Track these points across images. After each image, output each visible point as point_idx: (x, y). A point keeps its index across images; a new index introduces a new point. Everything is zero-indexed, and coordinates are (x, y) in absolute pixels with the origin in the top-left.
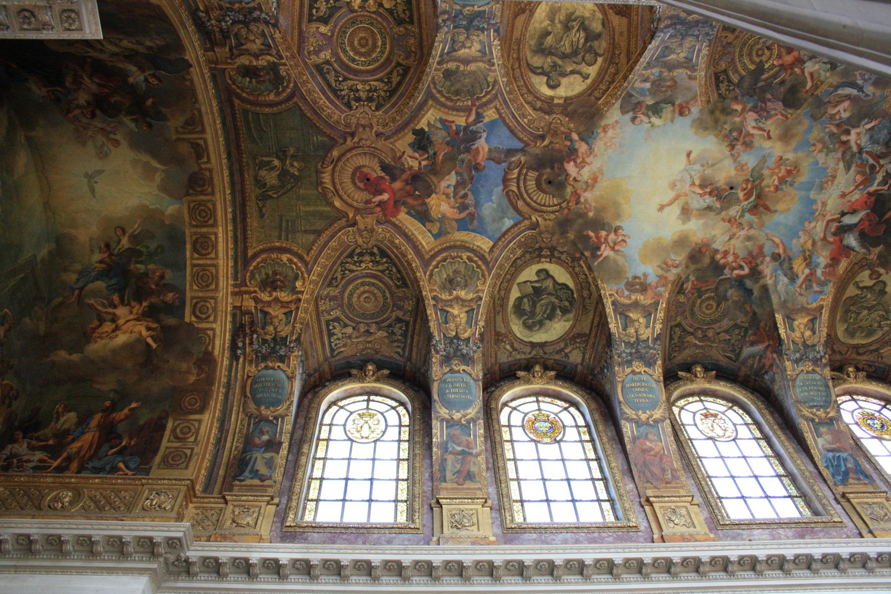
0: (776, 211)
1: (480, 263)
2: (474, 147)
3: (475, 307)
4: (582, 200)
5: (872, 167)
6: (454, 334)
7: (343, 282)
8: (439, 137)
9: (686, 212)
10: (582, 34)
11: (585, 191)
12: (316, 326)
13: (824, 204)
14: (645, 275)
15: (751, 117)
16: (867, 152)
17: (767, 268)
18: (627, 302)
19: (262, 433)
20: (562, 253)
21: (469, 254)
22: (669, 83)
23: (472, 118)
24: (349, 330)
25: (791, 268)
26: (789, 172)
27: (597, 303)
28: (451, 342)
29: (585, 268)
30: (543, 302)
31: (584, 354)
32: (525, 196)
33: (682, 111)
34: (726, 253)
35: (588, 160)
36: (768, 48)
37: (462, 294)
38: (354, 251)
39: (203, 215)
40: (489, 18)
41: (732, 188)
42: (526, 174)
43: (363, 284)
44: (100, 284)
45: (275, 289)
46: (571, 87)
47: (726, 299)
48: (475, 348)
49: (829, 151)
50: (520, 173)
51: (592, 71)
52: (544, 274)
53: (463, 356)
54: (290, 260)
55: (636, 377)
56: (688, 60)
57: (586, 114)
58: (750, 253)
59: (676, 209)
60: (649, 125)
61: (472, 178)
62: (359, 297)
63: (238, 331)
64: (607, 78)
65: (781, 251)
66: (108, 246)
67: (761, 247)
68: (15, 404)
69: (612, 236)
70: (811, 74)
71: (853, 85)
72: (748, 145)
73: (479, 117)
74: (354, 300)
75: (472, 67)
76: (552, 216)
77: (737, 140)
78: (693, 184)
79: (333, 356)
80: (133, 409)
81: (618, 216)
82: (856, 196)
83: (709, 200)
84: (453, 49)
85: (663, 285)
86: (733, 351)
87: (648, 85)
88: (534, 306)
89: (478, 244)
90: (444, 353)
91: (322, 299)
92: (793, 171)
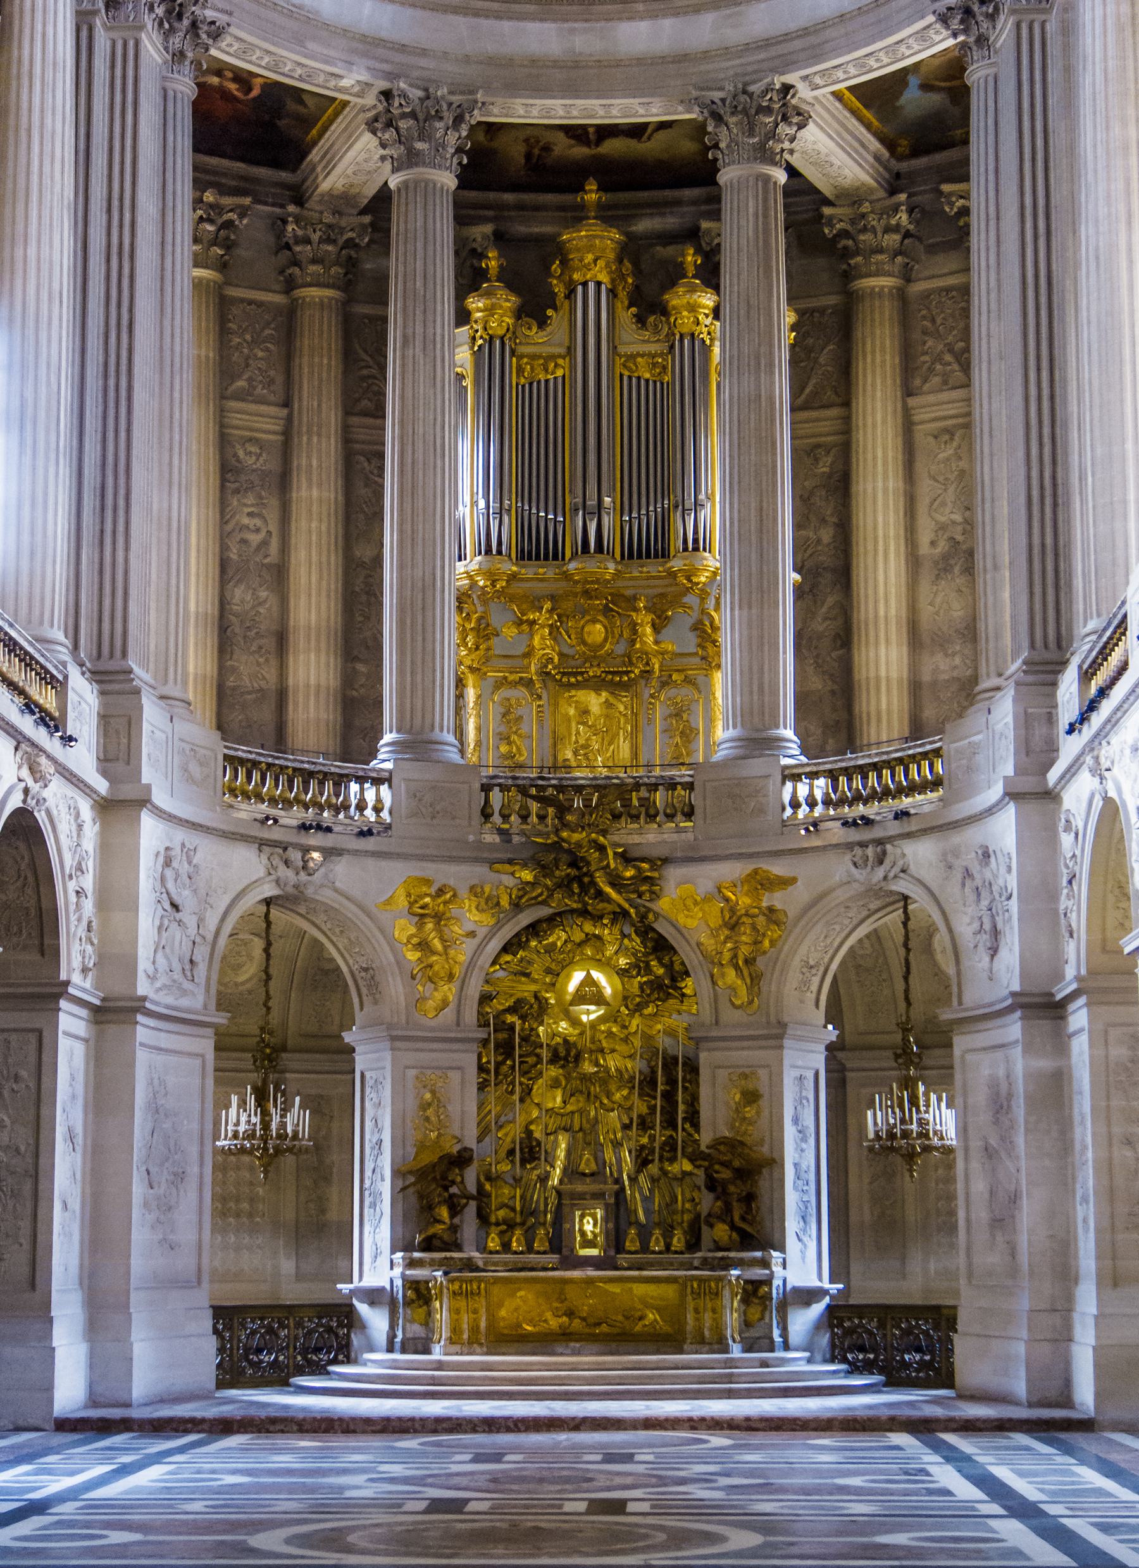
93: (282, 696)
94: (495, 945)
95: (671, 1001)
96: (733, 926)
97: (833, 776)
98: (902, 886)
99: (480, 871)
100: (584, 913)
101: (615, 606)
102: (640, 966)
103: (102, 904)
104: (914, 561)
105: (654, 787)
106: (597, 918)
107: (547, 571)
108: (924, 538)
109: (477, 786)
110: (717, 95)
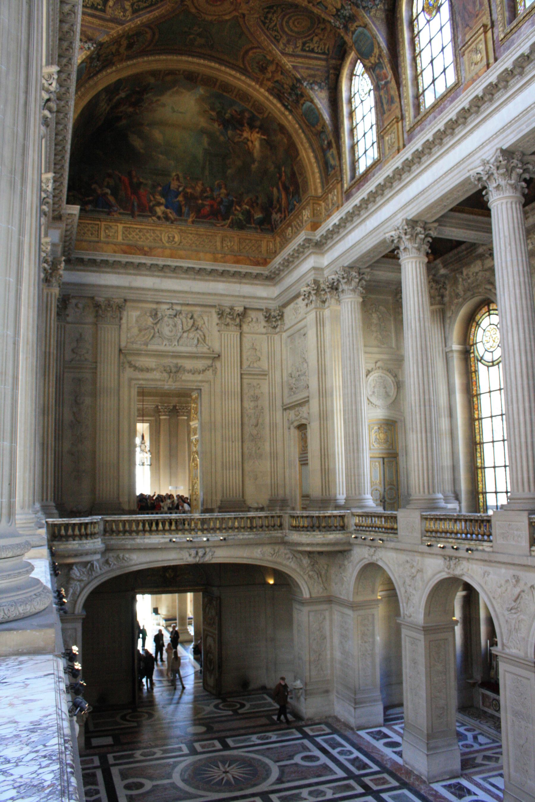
7: (281, 33)
12: (300, 60)
19: (324, 141)
24: (316, 39)
38: (262, 21)
39: (209, 81)
43: (287, 22)
44: (230, 132)
45: (266, 69)
53: (349, 18)
54: (254, 53)
62: (296, 26)
63: (280, 97)
66: (212, 119)
68: (259, 201)
74: (296, 30)
79: (328, 55)
80: (284, 172)
91: (284, 49)
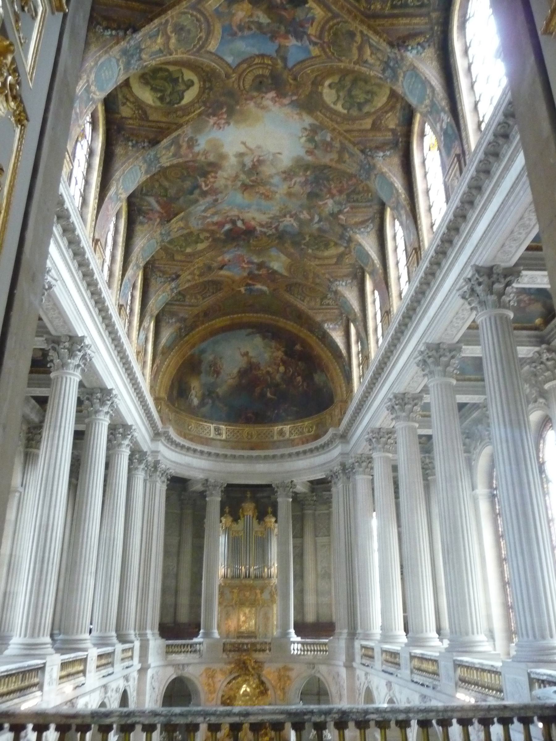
0: (243, 193)
1: (198, 46)
2: (290, 36)
3: (164, 53)
4: (248, 102)
5: (270, 227)
6: (143, 47)
8: (300, 14)
9: (241, 155)
10: (362, 100)
11: (255, 103)
13: (249, 212)
14: (199, 145)
15: (303, 179)
16: (279, 225)
17: (210, 199)
18: (181, 142)
20: (208, 94)
21: (204, 37)
22: (329, 149)
23: (313, 39)
25: (210, 208)
26: (268, 196)
27: (176, 124)
28: (137, 49)
29: (199, 111)
30: (166, 84)
31: (130, 118)
32: (250, 69)
33: (309, 152)
34: (216, 177)
35: (277, 104)
36: (341, 182)
37: (173, 41)
40: (392, 80)
41: (257, 174)
42: (267, 68)
46: (328, 95)
47: (183, 181)
48: (136, 67)
49: (280, 212)
50: (268, 65)
51: (339, 107)
52: (190, 84)
55: (139, 171)
56: (345, 162)
57: (310, 104)
58: (217, 189)
59: (242, 149)
60: (300, 135)
61: (265, 33)
64: (334, 117)
65: (219, 201)
67: (221, 192)
69: (223, 121)
70: (326, 203)
71: (320, 221)
72: (285, 179)
73: (315, 44)
75: (355, 51)
76: (236, 86)
77: (288, 175)
78: (260, 156)
81: (237, 122)
82: (253, 223)
83: (249, 164)
84: (371, 46)
85: (193, 156)
86: (148, 191)
87: (329, 139)
88: (162, 78)
89: (213, 42)
90: (128, 47)
92: (267, 197)
93: (176, 606)
94: (225, 683)
95: (265, 697)
96: (280, 679)
97: (303, 644)
98: (318, 675)
99: (221, 665)
100: (246, 674)
101: (252, 588)
102: (257, 687)
103: (138, 694)
104: (317, 576)
105: (262, 644)
106: (248, 675)
107: (237, 582)
108: (319, 570)
109: (222, 644)
110: (277, 482)
